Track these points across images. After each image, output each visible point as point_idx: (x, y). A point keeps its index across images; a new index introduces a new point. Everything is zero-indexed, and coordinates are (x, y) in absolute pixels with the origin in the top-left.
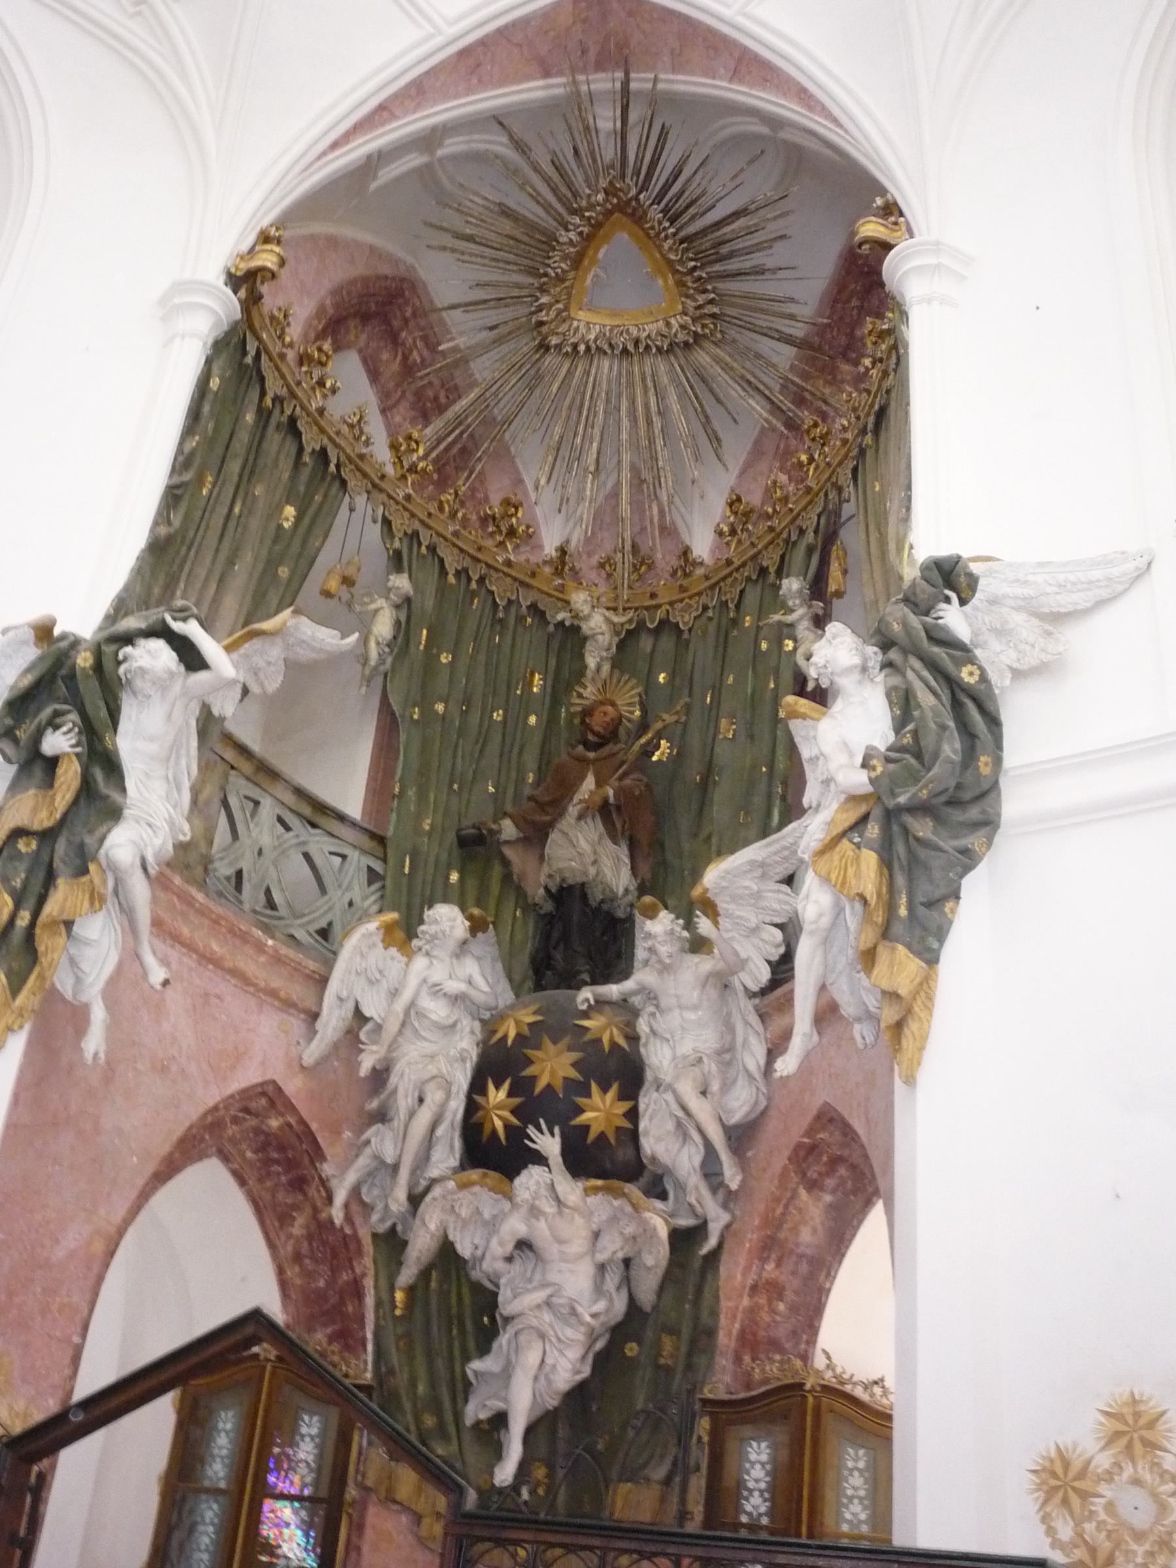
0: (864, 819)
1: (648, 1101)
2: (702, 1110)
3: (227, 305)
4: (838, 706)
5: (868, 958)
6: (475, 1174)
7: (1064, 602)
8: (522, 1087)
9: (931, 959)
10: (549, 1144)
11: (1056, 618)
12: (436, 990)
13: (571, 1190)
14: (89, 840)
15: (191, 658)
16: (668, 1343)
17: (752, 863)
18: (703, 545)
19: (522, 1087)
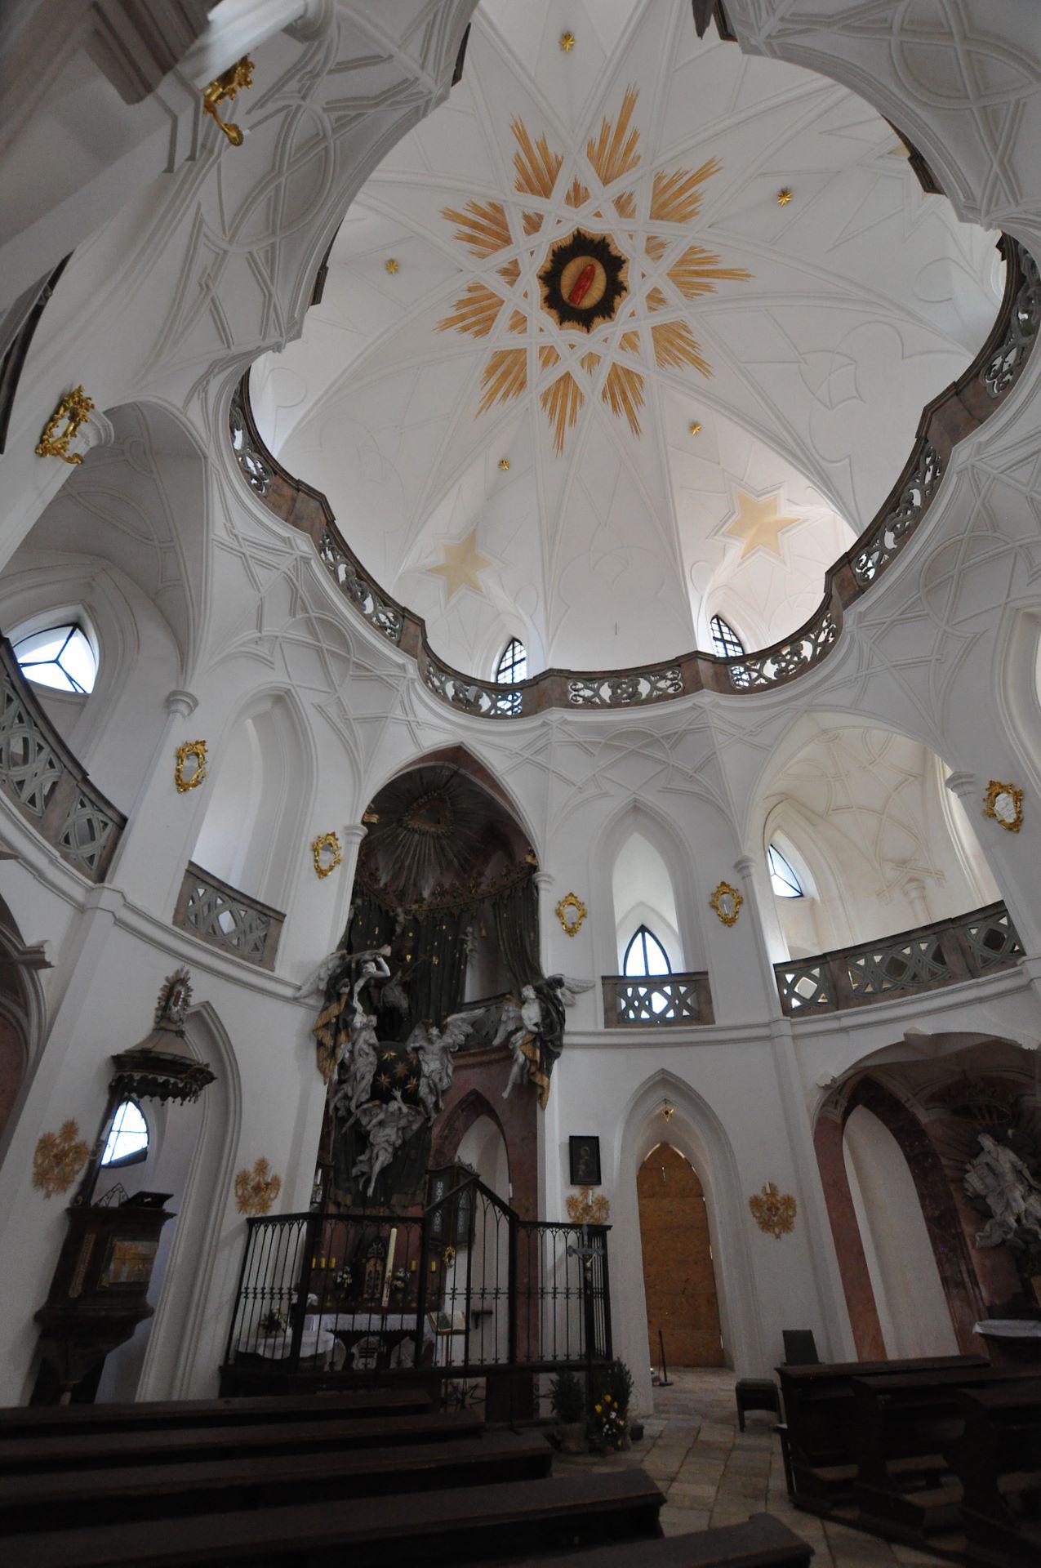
0: (535, 1038)
1: (423, 1081)
2: (439, 1086)
3: (363, 831)
4: (526, 1006)
5: (533, 1074)
6: (377, 1102)
7: (576, 989)
8: (392, 1076)
9: (549, 1077)
10: (398, 1094)
11: (573, 992)
12: (366, 1042)
13: (405, 1109)
14: (349, 1019)
15: (379, 967)
16: (413, 1152)
17: (462, 1018)
18: (426, 894)
19: (392, 1076)
